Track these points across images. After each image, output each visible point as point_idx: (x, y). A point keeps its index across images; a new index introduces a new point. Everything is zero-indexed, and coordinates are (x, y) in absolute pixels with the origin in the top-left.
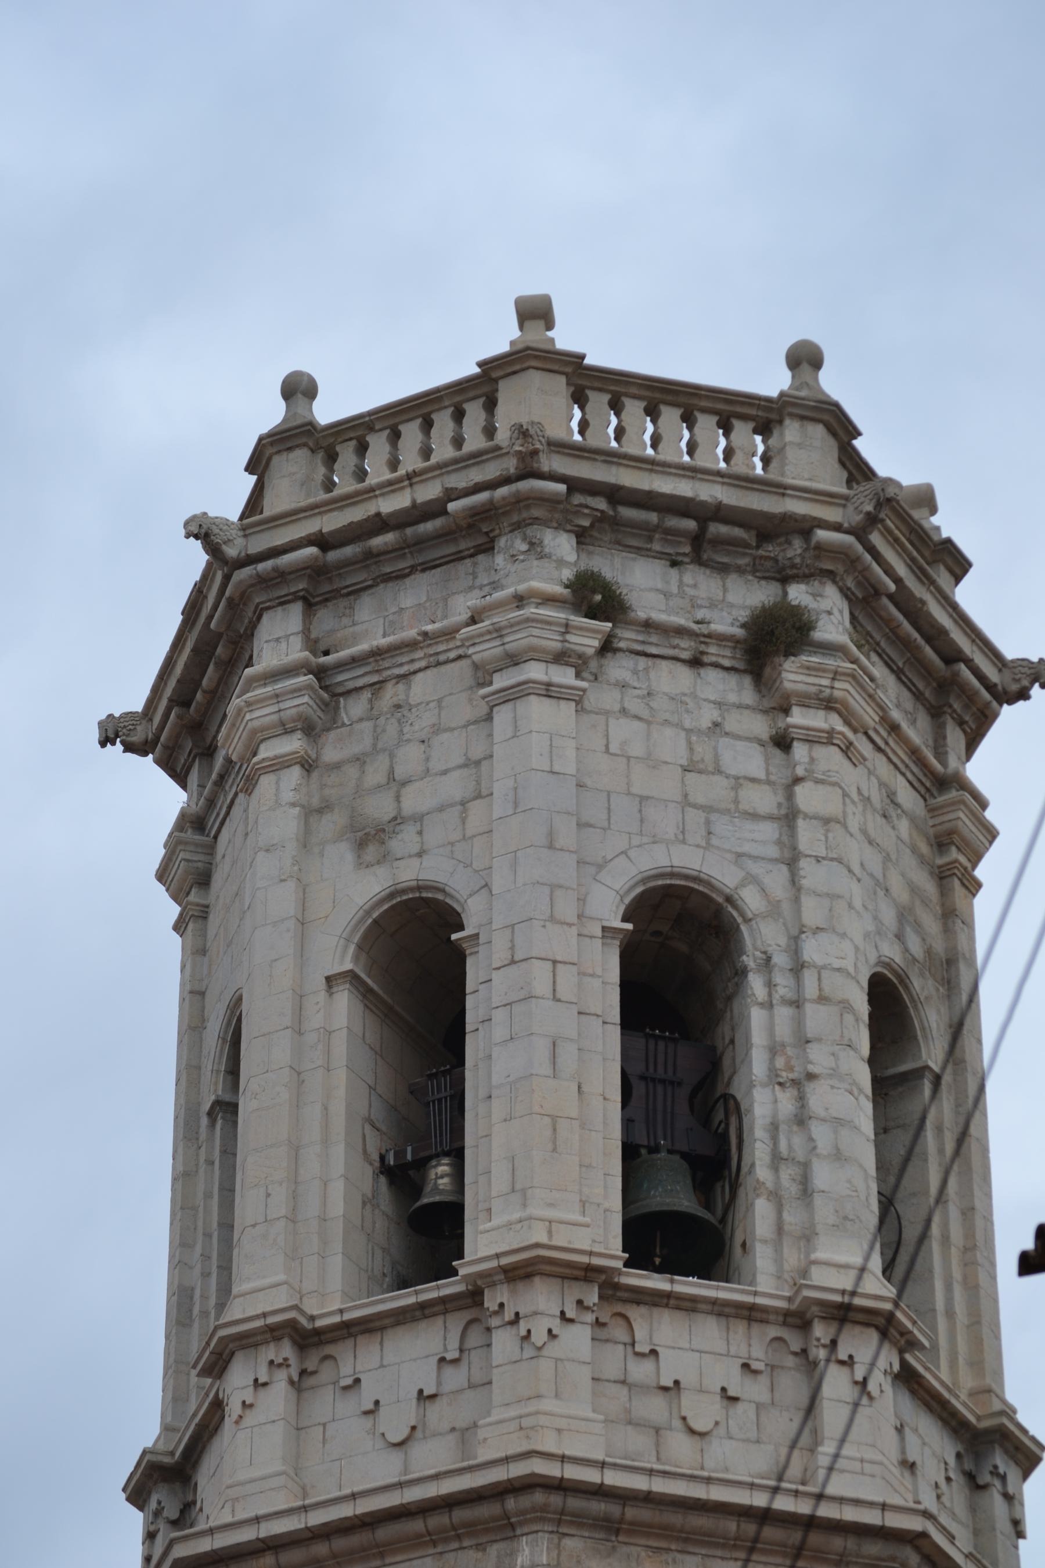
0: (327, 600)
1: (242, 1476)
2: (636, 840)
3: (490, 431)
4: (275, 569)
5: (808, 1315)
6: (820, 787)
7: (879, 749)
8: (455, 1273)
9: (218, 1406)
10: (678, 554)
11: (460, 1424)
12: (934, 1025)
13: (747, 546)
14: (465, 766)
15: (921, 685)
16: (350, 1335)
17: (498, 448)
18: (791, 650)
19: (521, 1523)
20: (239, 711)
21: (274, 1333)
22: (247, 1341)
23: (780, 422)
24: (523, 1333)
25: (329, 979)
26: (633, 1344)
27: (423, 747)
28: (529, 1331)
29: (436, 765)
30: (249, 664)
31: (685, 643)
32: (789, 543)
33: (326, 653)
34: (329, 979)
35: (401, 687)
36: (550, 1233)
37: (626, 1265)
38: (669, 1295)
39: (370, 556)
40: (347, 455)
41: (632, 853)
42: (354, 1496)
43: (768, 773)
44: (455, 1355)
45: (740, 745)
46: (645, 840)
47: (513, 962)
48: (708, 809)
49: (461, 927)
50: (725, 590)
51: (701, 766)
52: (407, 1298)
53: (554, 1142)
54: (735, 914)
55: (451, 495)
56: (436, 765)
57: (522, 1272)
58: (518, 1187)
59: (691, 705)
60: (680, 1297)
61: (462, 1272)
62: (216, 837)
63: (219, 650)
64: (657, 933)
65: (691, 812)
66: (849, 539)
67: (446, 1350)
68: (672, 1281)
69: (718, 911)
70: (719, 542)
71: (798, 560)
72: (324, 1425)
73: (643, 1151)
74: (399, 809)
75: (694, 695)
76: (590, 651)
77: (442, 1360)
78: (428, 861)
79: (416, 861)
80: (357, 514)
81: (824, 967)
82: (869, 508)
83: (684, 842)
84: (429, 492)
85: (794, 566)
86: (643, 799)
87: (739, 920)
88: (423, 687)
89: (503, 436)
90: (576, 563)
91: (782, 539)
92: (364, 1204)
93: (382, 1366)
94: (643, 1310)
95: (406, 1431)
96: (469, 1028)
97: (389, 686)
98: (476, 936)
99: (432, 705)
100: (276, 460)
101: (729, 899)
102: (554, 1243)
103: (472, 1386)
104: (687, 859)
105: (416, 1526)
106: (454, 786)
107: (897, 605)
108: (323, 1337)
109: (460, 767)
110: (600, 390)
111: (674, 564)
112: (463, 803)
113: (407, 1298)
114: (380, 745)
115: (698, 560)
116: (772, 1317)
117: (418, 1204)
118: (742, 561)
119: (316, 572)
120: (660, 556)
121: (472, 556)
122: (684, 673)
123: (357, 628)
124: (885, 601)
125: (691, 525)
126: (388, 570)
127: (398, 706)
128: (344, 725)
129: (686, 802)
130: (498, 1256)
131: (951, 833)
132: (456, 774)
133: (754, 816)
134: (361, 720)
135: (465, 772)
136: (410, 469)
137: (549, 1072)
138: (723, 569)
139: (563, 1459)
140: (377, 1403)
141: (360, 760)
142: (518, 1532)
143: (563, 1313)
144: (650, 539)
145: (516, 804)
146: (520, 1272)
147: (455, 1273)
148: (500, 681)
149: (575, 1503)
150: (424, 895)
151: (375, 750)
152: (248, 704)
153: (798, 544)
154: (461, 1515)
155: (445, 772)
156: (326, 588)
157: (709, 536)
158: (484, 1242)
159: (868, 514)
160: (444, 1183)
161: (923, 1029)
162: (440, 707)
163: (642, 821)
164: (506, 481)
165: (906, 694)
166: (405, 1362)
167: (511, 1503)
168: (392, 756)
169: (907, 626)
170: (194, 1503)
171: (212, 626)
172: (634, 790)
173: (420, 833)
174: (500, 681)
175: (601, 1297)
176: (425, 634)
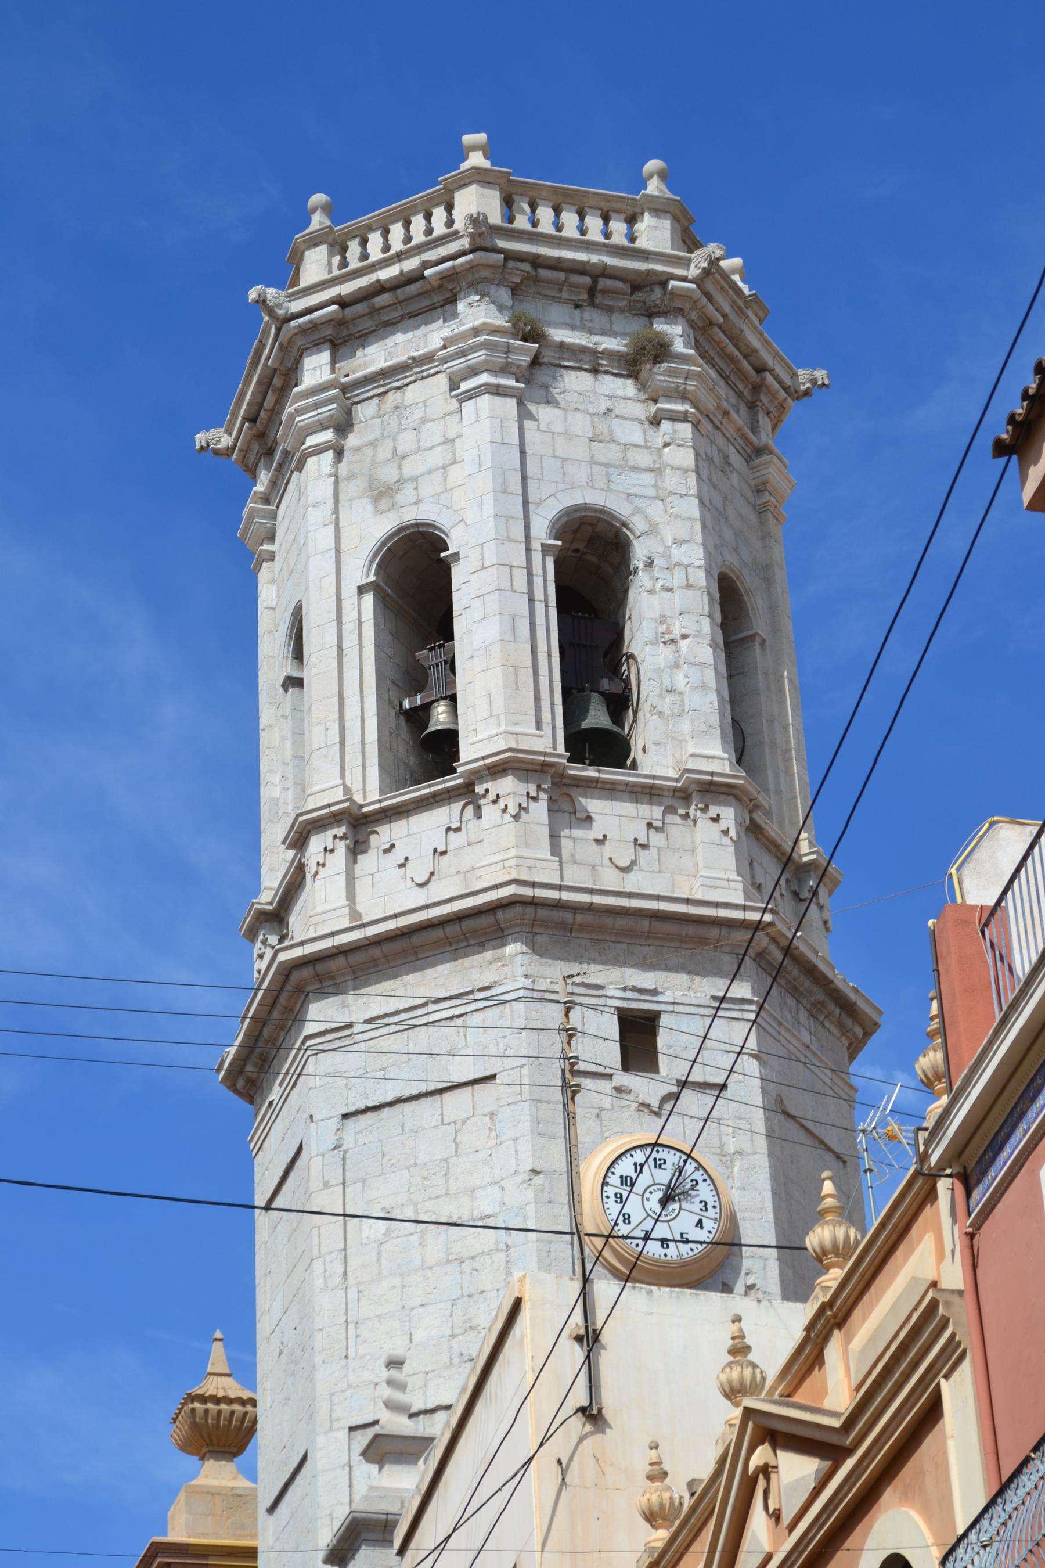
0: (345, 341)
1: (320, 909)
2: (561, 487)
3: (450, 223)
4: (310, 321)
5: (690, 790)
6: (681, 448)
7: (717, 428)
8: (454, 771)
9: (301, 868)
10: (579, 300)
11: (462, 869)
12: (760, 607)
13: (625, 294)
14: (444, 443)
15: (741, 387)
16: (387, 816)
17: (457, 232)
18: (657, 359)
19: (507, 928)
20: (292, 417)
21: (335, 819)
22: (319, 825)
23: (642, 214)
24: (503, 807)
25: (359, 588)
26: (575, 813)
27: (415, 432)
28: (506, 806)
29: (424, 444)
30: (296, 385)
31: (586, 358)
32: (652, 290)
33: (347, 376)
34: (359, 588)
35: (399, 394)
36: (517, 742)
37: (568, 762)
38: (597, 780)
39: (375, 311)
40: (354, 248)
41: (558, 495)
42: (396, 916)
43: (646, 441)
44: (458, 825)
45: (627, 423)
46: (567, 486)
47: (483, 568)
48: (606, 465)
49: (447, 549)
50: (611, 323)
51: (601, 438)
52: (423, 790)
53: (517, 683)
54: (628, 533)
55: (426, 265)
56: (424, 444)
57: (500, 768)
58: (494, 713)
59: (593, 399)
60: (605, 782)
61: (459, 770)
62: (278, 507)
63: (275, 380)
64: (577, 551)
65: (596, 468)
66: (694, 286)
67: (451, 822)
68: (599, 771)
69: (618, 533)
70: (605, 292)
71: (658, 302)
72: (372, 875)
73: (574, 692)
74: (401, 474)
75: (594, 391)
76: (525, 364)
77: (449, 829)
78: (422, 507)
79: (414, 507)
80: (363, 282)
81: (690, 565)
82: (705, 265)
83: (592, 487)
84: (411, 264)
85: (656, 306)
86: (564, 460)
87: (632, 537)
88: (414, 393)
89: (459, 225)
90: (512, 307)
91: (648, 289)
92: (391, 733)
93: (409, 835)
94: (580, 790)
95: (428, 875)
96: (455, 614)
97: (390, 394)
98: (458, 553)
99: (420, 405)
100: (307, 253)
101: (625, 525)
102: (520, 747)
103: (469, 844)
104: (595, 498)
105: (439, 933)
106: (436, 457)
107: (724, 332)
108: (369, 819)
109: (440, 444)
110: (522, 195)
111: (577, 306)
112: (444, 468)
113: (423, 790)
114: (386, 433)
115: (592, 303)
116: (665, 793)
117: (427, 732)
118: (622, 304)
119: (339, 323)
120: (567, 301)
121: (441, 306)
123: (367, 358)
124: (716, 329)
125: (587, 280)
126: (386, 319)
127: (397, 408)
128: (361, 422)
129: (592, 461)
130: (483, 758)
131: (765, 483)
132: (438, 449)
133: (636, 469)
134: (373, 418)
135: (445, 447)
136: (398, 250)
137: (511, 638)
138: (609, 310)
139: (534, 885)
140: (407, 859)
141: (373, 444)
142: (506, 933)
143: (528, 793)
144: (561, 290)
145: (480, 465)
146: (497, 770)
147: (454, 771)
148: (465, 386)
149: (542, 913)
150: (421, 530)
151: (383, 437)
153: (658, 291)
154: (467, 924)
155: (431, 448)
156: (345, 333)
157: (599, 287)
158: (471, 751)
159: (704, 269)
160: (442, 717)
161: (753, 609)
162: (425, 406)
163: (564, 474)
164: (463, 253)
165: (731, 392)
166: (426, 829)
167: (500, 914)
168: (394, 440)
169: (731, 348)
170: (287, 934)
172: (558, 454)
173: (416, 489)
174: (465, 386)
175: (552, 783)
176: (413, 358)
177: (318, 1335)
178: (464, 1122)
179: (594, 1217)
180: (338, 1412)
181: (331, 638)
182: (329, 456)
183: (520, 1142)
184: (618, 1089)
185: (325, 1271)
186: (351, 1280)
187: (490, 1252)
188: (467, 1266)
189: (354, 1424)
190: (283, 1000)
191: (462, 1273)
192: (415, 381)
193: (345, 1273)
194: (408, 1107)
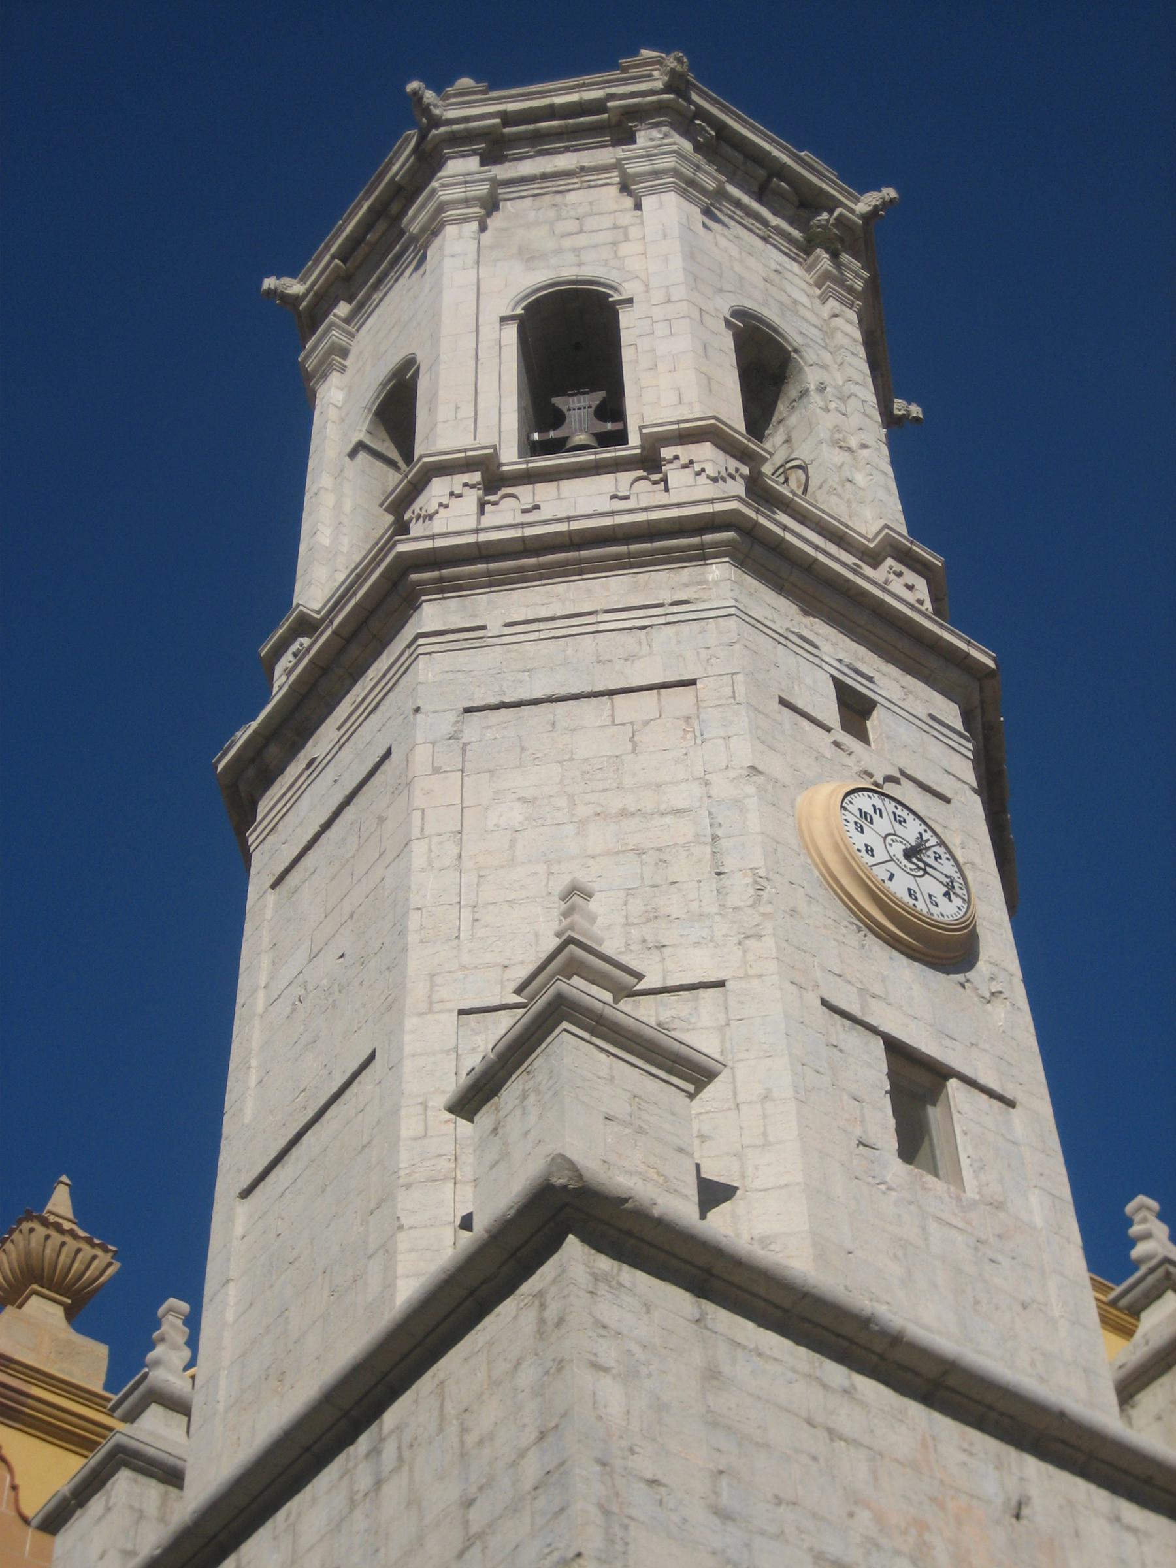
4: (466, 130)
21: (467, 465)
55: (612, 97)
62: (358, 330)
101: (796, 351)
112: (614, 244)
122: (759, 243)
152: (443, 185)
157: (772, 185)
164: (652, 92)
167: (708, 538)
171: (397, 179)
177: (414, 917)
178: (646, 723)
179: (832, 835)
181: (469, 343)
182: (475, 225)
184: (837, 744)
185: (430, 851)
186: (467, 863)
191: (642, 864)
192: (579, 189)
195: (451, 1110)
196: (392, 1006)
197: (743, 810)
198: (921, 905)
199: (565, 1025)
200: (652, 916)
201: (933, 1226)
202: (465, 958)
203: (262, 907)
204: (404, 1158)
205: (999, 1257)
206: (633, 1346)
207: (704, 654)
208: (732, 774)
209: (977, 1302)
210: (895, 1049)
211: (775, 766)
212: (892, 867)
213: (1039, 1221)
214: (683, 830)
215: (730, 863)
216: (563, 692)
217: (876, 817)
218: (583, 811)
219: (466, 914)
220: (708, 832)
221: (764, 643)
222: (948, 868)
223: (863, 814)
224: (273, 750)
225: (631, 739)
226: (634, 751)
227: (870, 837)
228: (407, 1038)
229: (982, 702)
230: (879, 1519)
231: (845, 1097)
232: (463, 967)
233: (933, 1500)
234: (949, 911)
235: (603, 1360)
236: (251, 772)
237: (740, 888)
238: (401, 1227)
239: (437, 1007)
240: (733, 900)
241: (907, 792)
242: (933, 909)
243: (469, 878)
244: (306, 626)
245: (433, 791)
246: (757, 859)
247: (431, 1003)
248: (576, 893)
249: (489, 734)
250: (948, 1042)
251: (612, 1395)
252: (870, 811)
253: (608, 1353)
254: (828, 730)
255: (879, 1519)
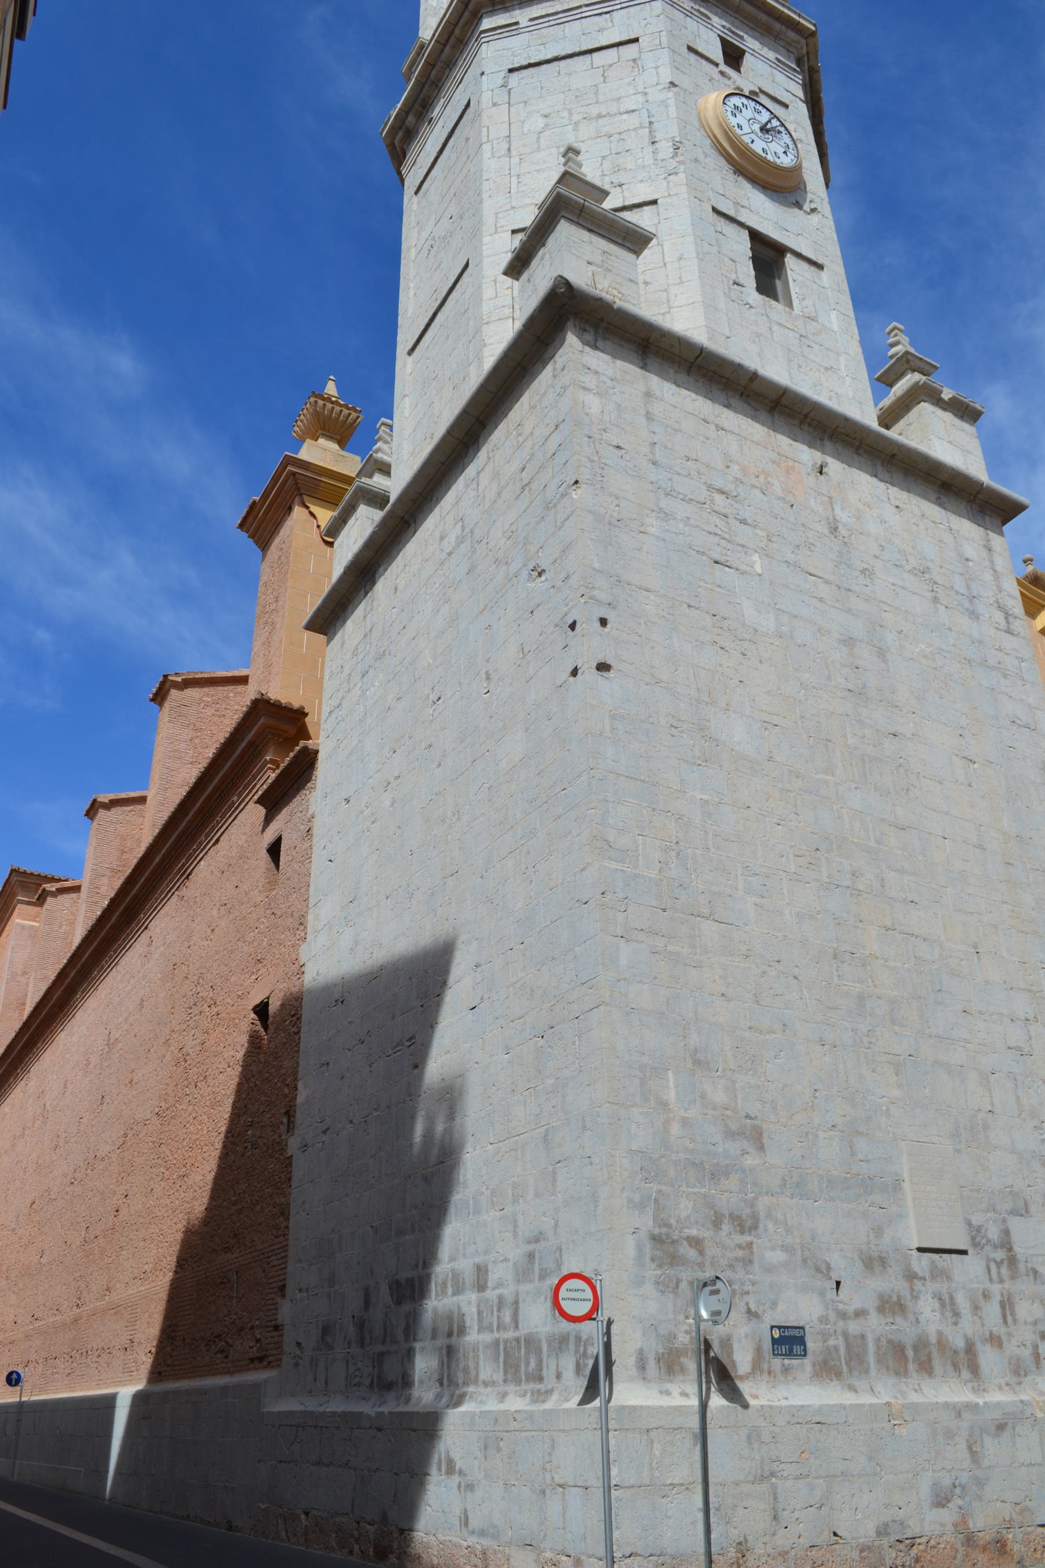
179: (718, 118)
180: (502, 222)
183: (660, 70)
184: (722, 73)
186: (514, 152)
187: (635, 129)
188: (615, 138)
189: (516, 227)
190: (457, 31)
193: (509, 150)
194: (563, 63)
195: (505, 273)
196: (476, 233)
197: (667, 107)
198: (770, 157)
199: (563, 213)
200: (617, 169)
201: (775, 327)
202: (514, 203)
203: (411, 204)
204: (485, 308)
205: (813, 345)
206: (604, 378)
207: (643, 23)
208: (660, 87)
209: (800, 367)
210: (755, 236)
211: (684, 82)
212: (753, 136)
213: (836, 328)
214: (633, 121)
215: (659, 136)
216: (563, 53)
217: (744, 110)
218: (576, 118)
219: (514, 180)
220: (647, 121)
221: (678, 16)
222: (786, 139)
223: (736, 107)
224: (411, 119)
225: (603, 75)
226: (604, 81)
227: (740, 119)
228: (484, 248)
229: (808, 53)
230: (744, 469)
231: (726, 259)
232: (513, 208)
233: (773, 462)
234: (787, 161)
235: (587, 385)
236: (400, 134)
237: (665, 149)
238: (485, 345)
239: (500, 230)
240: (661, 156)
241: (763, 99)
242: (777, 160)
243: (515, 160)
244: (422, 47)
245: (493, 120)
246: (674, 131)
247: (496, 228)
248: (571, 152)
249: (523, 82)
250: (784, 232)
251: (593, 404)
252: (741, 106)
253: (590, 381)
254: (717, 65)
255: (744, 469)
